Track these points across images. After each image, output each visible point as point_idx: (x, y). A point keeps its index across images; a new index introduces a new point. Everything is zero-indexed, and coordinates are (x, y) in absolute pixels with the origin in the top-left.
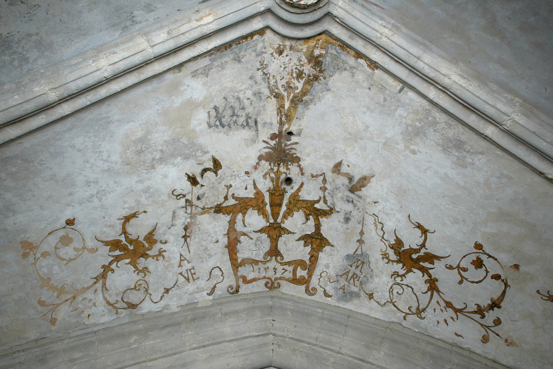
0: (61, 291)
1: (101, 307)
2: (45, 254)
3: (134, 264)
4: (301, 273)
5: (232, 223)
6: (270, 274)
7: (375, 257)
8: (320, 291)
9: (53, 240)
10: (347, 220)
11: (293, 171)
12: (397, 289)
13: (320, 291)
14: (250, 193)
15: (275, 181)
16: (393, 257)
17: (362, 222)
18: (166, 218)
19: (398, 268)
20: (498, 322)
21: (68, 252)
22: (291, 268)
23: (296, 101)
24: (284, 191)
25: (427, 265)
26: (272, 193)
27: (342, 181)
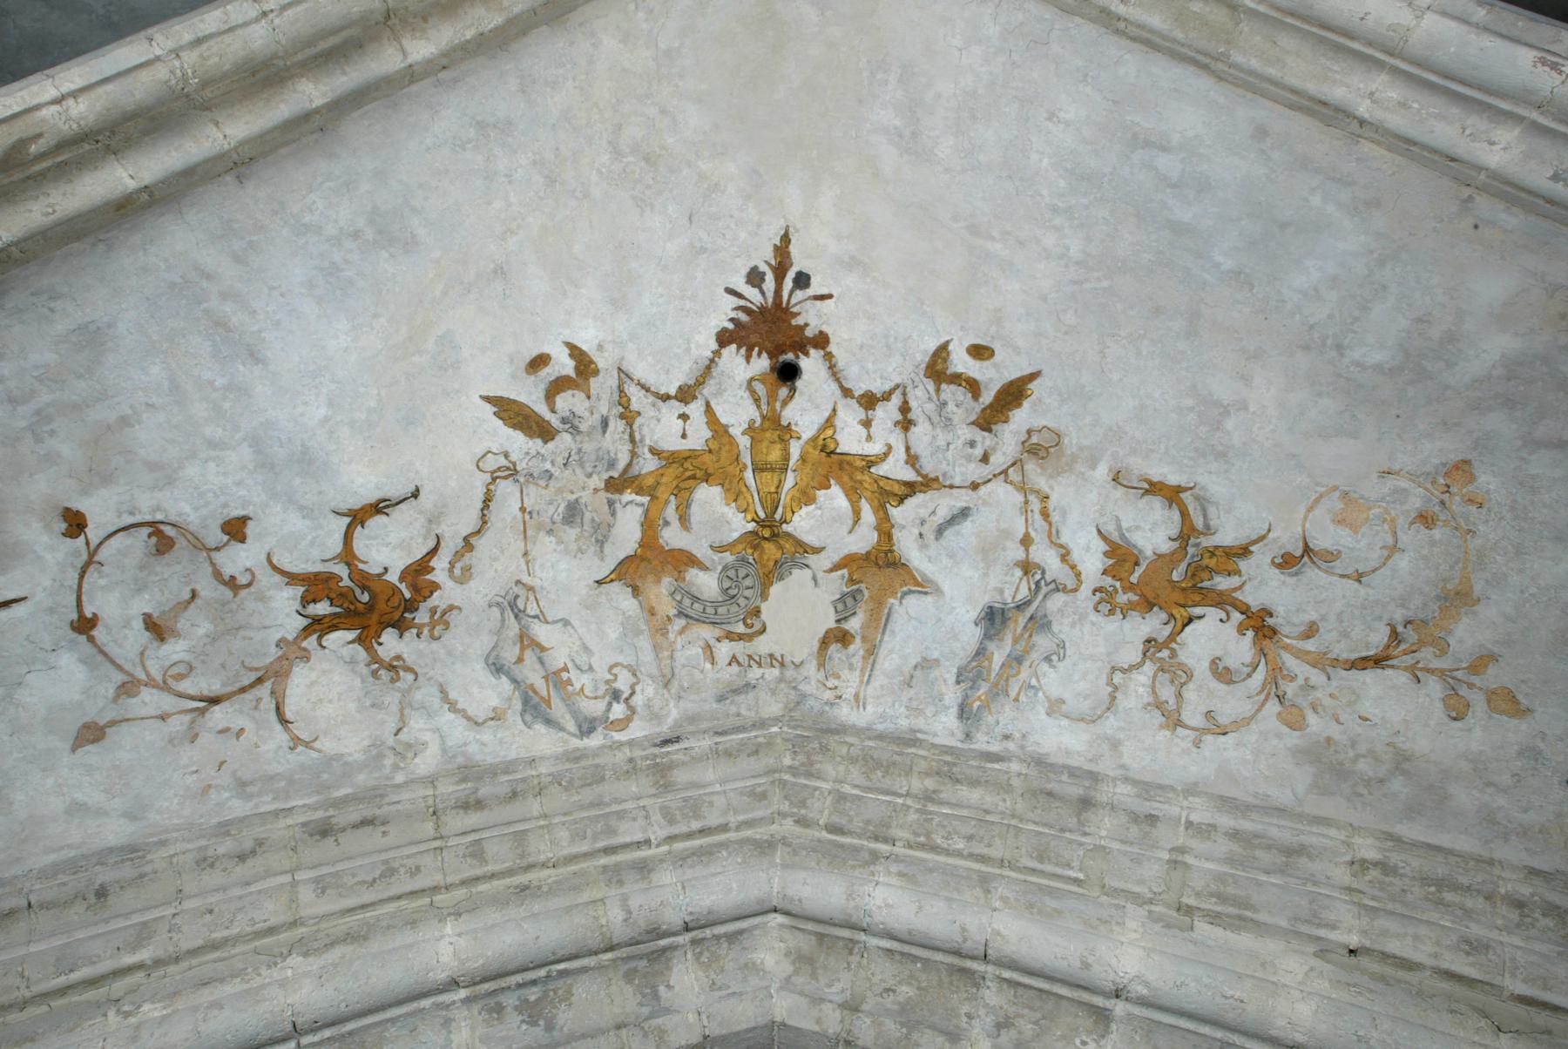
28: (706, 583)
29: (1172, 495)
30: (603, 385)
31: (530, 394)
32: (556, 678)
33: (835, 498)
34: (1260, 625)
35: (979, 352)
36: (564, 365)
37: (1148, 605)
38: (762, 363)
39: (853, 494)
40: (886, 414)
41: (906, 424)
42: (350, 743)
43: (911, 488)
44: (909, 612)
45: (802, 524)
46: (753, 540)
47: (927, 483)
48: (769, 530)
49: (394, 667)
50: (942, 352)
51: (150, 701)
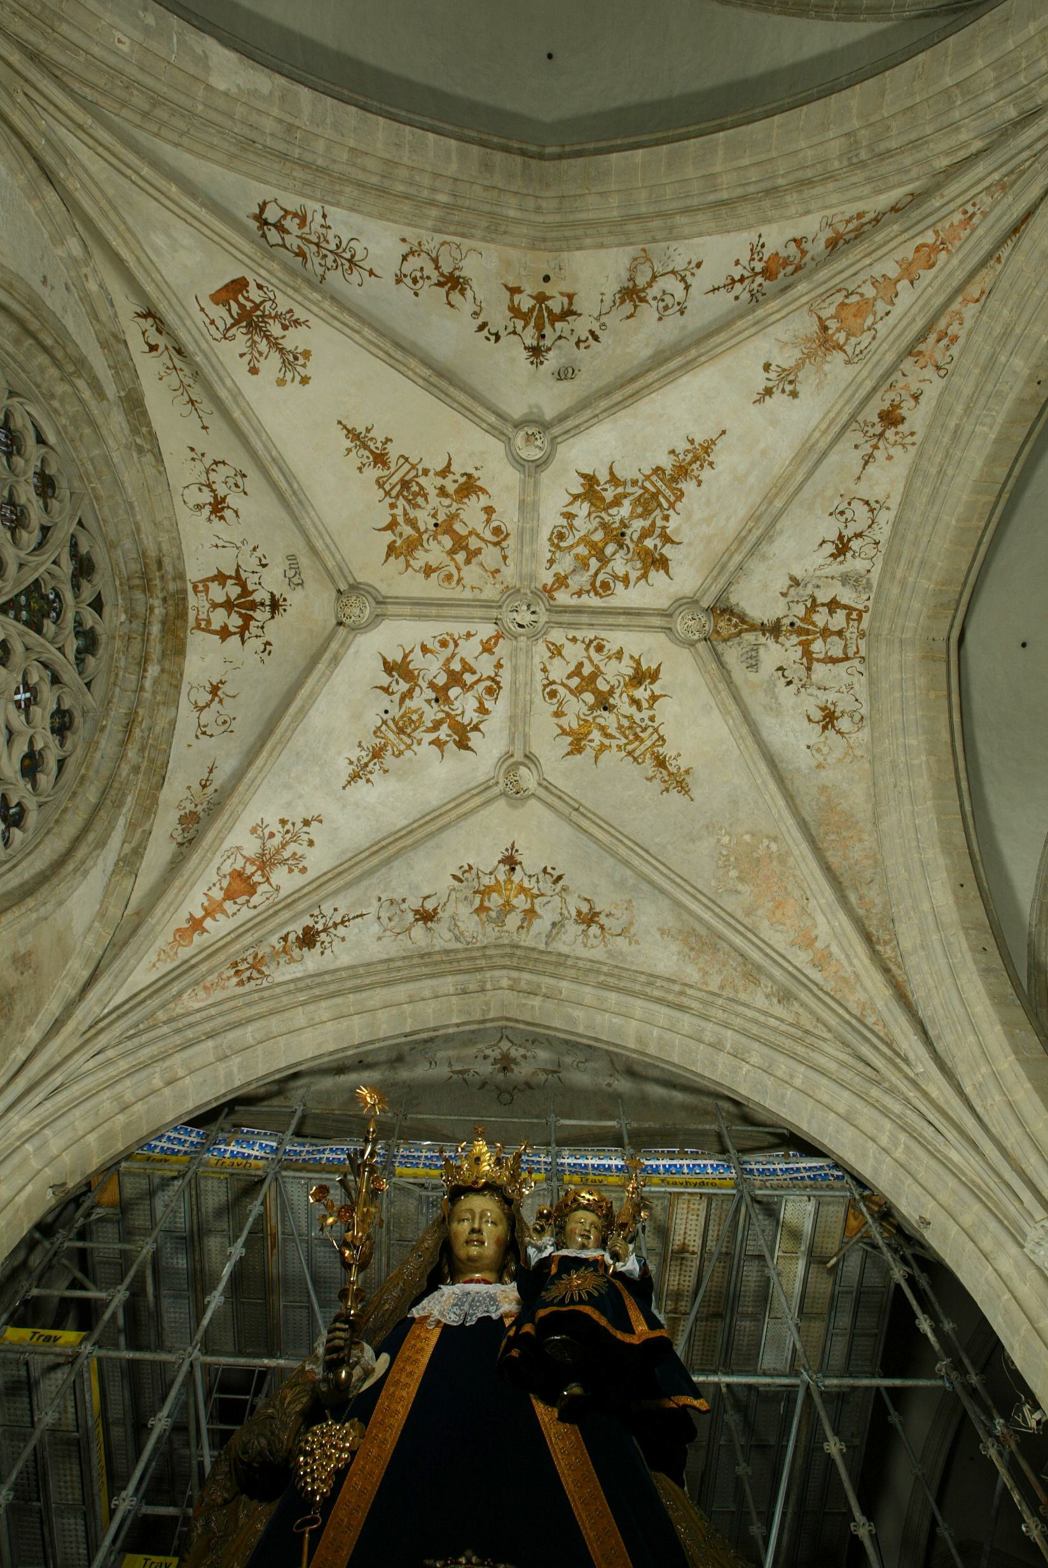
0: (847, 754)
1: (860, 734)
2: (825, 760)
3: (837, 719)
4: (854, 616)
5: (818, 660)
6: (854, 636)
7: (843, 568)
8: (867, 603)
9: (817, 756)
10: (818, 587)
11: (786, 621)
12: (863, 555)
13: (867, 603)
14: (800, 649)
15: (791, 633)
16: (842, 558)
17: (819, 578)
18: (812, 699)
19: (849, 555)
20: (877, 502)
21: (825, 750)
22: (851, 623)
23: (743, 621)
24: (799, 627)
25: (845, 539)
26: (799, 634)
27: (792, 591)
28: (493, 914)
29: (588, 901)
30: (474, 872)
31: (459, 874)
32: (461, 933)
33: (522, 897)
34: (602, 927)
35: (553, 869)
36: (466, 868)
37: (583, 922)
38: (508, 867)
39: (526, 896)
40: (534, 879)
41: (538, 882)
42: (423, 944)
43: (538, 896)
44: (537, 922)
45: (514, 902)
46: (504, 905)
47: (542, 895)
48: (508, 903)
49: (430, 929)
50: (545, 868)
51: (388, 933)
